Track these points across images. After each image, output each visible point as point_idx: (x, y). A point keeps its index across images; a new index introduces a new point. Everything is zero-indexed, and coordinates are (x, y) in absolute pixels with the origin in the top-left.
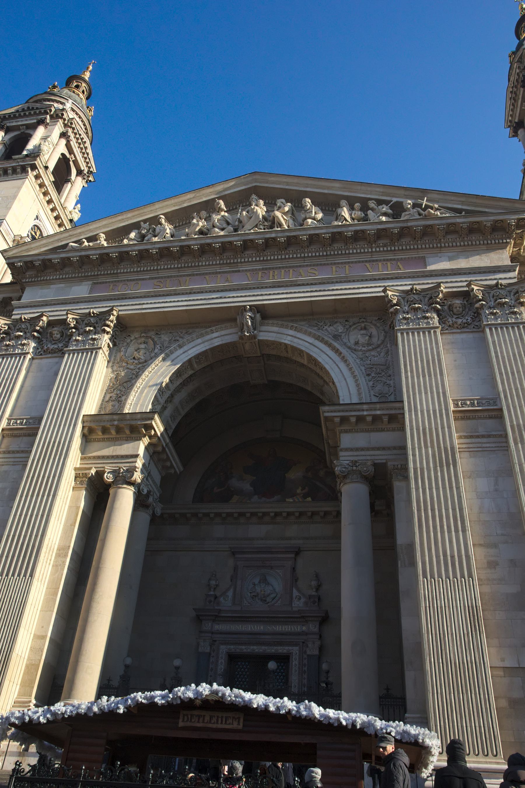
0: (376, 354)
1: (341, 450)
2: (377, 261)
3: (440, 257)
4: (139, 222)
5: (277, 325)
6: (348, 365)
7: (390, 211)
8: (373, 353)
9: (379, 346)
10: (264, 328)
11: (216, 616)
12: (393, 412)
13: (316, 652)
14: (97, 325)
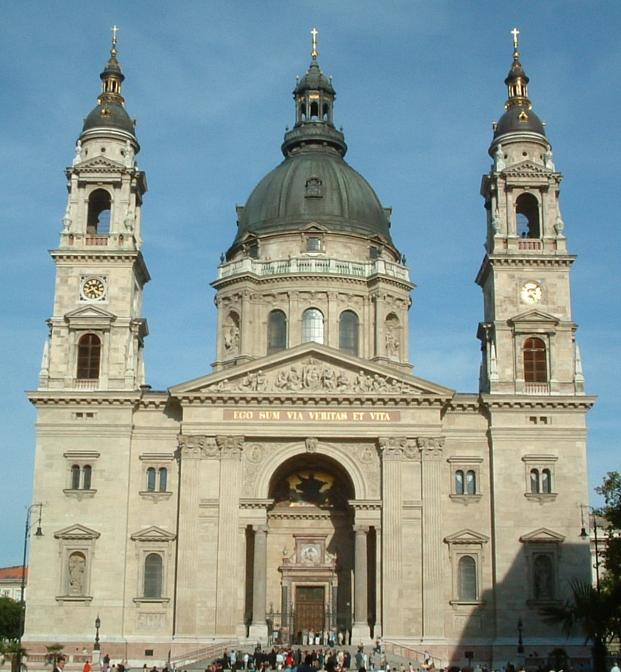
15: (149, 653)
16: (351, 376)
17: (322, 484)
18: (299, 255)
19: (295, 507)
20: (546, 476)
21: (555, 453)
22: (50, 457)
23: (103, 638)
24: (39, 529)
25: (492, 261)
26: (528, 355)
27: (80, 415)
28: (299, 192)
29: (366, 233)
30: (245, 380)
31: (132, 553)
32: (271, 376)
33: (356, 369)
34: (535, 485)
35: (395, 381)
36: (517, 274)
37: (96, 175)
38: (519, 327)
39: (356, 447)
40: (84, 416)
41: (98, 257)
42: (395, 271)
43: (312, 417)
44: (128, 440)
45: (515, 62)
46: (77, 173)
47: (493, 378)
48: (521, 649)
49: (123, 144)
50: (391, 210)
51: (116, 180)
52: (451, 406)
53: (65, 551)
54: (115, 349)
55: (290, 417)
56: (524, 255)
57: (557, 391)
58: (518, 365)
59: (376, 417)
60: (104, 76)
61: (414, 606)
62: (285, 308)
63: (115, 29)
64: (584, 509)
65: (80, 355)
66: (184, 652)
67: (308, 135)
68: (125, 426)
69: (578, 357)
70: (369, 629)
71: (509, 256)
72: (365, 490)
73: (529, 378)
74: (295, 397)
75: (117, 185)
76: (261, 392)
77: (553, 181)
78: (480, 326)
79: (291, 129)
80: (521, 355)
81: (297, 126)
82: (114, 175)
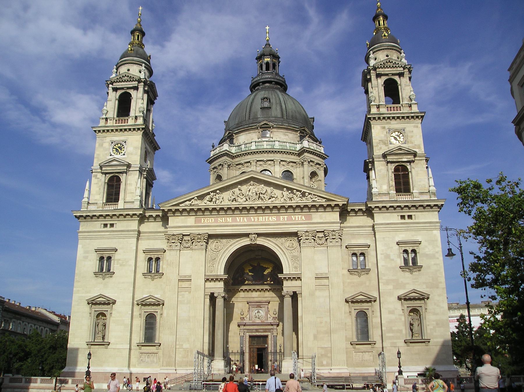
2: (296, 215)
4: (209, 192)
7: (301, 195)
8: (294, 251)
10: (258, 239)
16: (277, 193)
17: (265, 269)
18: (257, 140)
20: (413, 255)
22: (86, 252)
25: (370, 118)
26: (397, 177)
27: (105, 225)
28: (258, 104)
29: (297, 127)
30: (208, 197)
32: (227, 195)
34: (406, 261)
35: (307, 194)
36: (387, 126)
37: (123, 83)
38: (390, 158)
39: (283, 240)
40: (109, 225)
42: (314, 146)
43: (253, 220)
46: (112, 84)
47: (374, 191)
49: (141, 67)
51: (134, 85)
54: (130, 184)
55: (238, 220)
56: (390, 114)
57: (417, 198)
58: (391, 182)
61: (326, 346)
63: (140, 8)
64: (450, 232)
65: (108, 189)
68: (133, 231)
69: (431, 175)
71: (381, 114)
72: (289, 267)
73: (398, 190)
74: (241, 207)
75: (136, 88)
77: (406, 70)
78: (365, 161)
81: (258, 75)
82: (134, 83)
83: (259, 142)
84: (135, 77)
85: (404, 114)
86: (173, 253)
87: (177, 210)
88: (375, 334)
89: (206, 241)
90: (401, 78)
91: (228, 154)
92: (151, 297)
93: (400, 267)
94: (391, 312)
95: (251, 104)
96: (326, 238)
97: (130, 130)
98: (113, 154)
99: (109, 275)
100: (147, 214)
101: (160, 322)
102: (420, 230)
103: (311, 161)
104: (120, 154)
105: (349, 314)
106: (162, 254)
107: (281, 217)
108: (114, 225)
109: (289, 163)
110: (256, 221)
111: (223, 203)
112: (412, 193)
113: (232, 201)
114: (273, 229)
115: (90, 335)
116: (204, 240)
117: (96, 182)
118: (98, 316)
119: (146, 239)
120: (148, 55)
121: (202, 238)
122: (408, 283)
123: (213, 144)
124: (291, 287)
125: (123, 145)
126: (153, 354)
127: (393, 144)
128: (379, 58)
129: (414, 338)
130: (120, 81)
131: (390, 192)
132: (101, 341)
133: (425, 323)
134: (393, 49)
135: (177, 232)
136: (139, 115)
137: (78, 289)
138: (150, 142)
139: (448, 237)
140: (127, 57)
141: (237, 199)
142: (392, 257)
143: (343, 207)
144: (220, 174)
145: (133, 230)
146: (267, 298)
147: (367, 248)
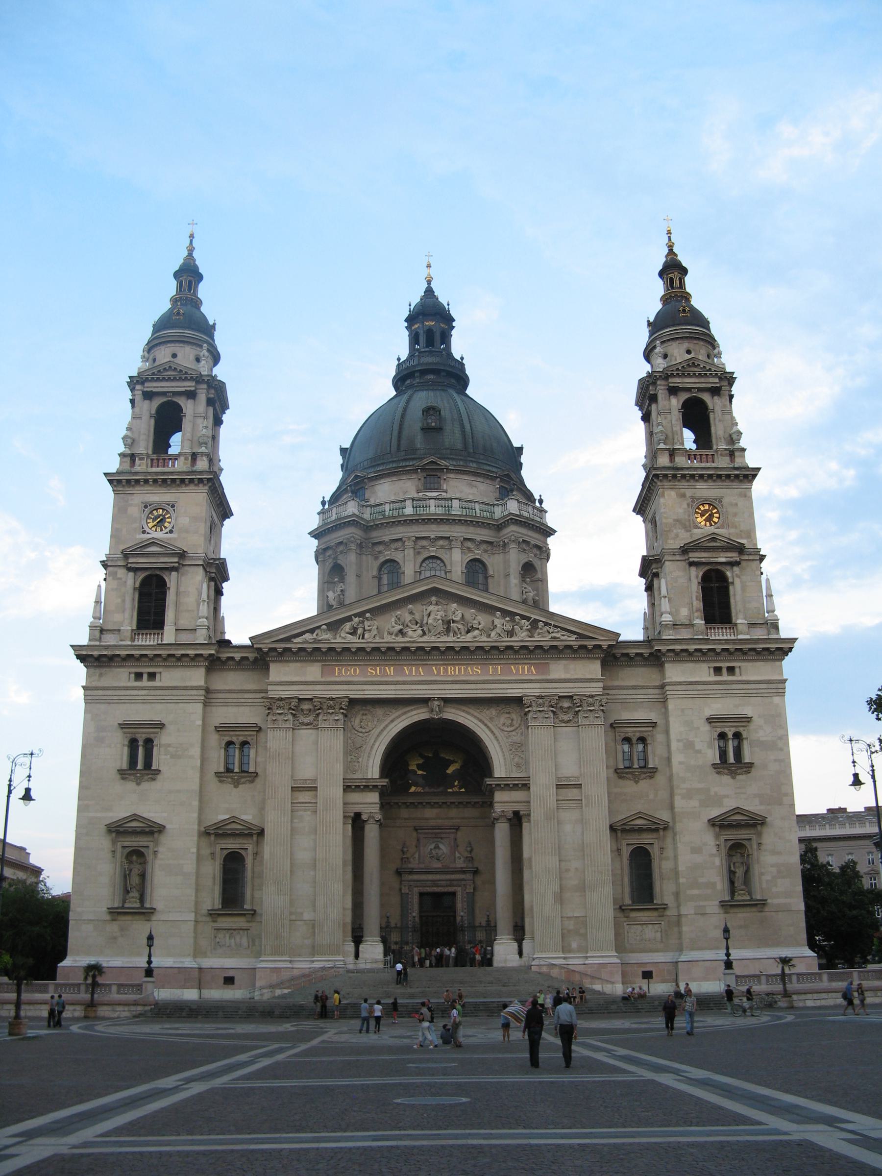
0: (516, 734)
1: (496, 802)
3: (559, 664)
5: (454, 708)
6: (499, 743)
7: (529, 627)
8: (514, 733)
9: (517, 728)
10: (446, 709)
11: (411, 872)
12: (524, 782)
13: (472, 891)
14: (336, 707)
15: (229, 981)
16: (482, 619)
18: (416, 495)
19: (414, 793)
21: (748, 711)
23: (156, 962)
24: (28, 790)
25: (656, 476)
27: (139, 676)
29: (494, 470)
30: (348, 626)
31: (206, 852)
33: (490, 609)
34: (723, 754)
35: (541, 624)
36: (689, 493)
38: (695, 556)
39: (493, 712)
40: (145, 677)
41: (164, 481)
43: (436, 673)
44: (200, 706)
45: (671, 252)
46: (143, 383)
48: (729, 965)
49: (198, 349)
50: (520, 450)
52: (614, 656)
53: (119, 849)
56: (696, 469)
59: (518, 670)
60: (177, 275)
62: (398, 557)
64: (856, 746)
65: (140, 602)
66: (274, 979)
67: (422, 364)
70: (515, 945)
76: (370, 639)
77: (726, 383)
78: (644, 558)
79: (404, 357)
80: (695, 589)
83: (419, 500)
84: (190, 372)
85: (721, 471)
86: (279, 734)
87: (286, 650)
88: (664, 891)
89: (344, 712)
90: (716, 398)
91: (358, 522)
92: (233, 820)
93: (713, 764)
94: (696, 850)
95: (402, 417)
96: (577, 709)
97: (182, 481)
98: (148, 530)
99: (150, 776)
100: (224, 656)
101: (253, 869)
102: (748, 695)
103: (524, 541)
104: (161, 530)
105: (617, 853)
106: (253, 735)
107: (491, 667)
108: (158, 676)
109: (480, 543)
110: (442, 674)
111: (377, 640)
112: (736, 624)
113: (396, 635)
114: (475, 692)
115: (114, 895)
116: (342, 711)
117: (115, 587)
118: (129, 855)
119: (222, 704)
120: (211, 323)
121: (337, 707)
122: (727, 796)
123: (324, 498)
124: (510, 802)
125: (168, 512)
126: (241, 932)
127: (699, 528)
128: (672, 356)
129: (736, 898)
130: (158, 380)
131: (695, 622)
132: (138, 906)
133: (756, 870)
134: (699, 339)
135: (287, 693)
136: (200, 450)
137: (86, 802)
138: (218, 505)
139: (853, 754)
140: (173, 327)
141: (405, 631)
142: (697, 748)
143: (609, 650)
144: (339, 562)
145: (196, 687)
146: (454, 821)
147: (651, 728)
